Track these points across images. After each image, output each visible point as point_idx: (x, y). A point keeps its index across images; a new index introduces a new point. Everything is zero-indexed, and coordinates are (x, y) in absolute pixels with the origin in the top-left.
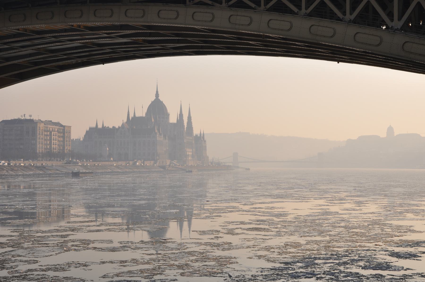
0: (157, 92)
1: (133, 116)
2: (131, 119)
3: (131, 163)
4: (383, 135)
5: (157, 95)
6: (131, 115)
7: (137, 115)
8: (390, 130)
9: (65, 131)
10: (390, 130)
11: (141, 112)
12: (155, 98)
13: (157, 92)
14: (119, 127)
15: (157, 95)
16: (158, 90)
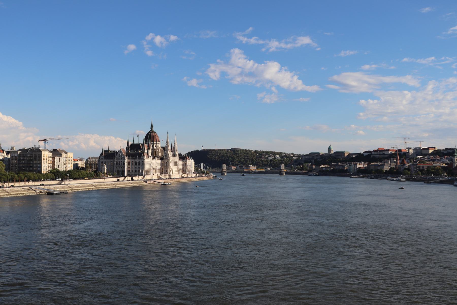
0: (152, 125)
1: (132, 143)
2: (130, 145)
3: (121, 179)
4: (326, 151)
5: (152, 127)
6: (130, 143)
7: (135, 142)
8: (330, 149)
9: (68, 157)
10: (330, 149)
11: (140, 140)
12: (150, 129)
13: (152, 125)
14: (118, 151)
15: (152, 127)
16: (153, 124)
